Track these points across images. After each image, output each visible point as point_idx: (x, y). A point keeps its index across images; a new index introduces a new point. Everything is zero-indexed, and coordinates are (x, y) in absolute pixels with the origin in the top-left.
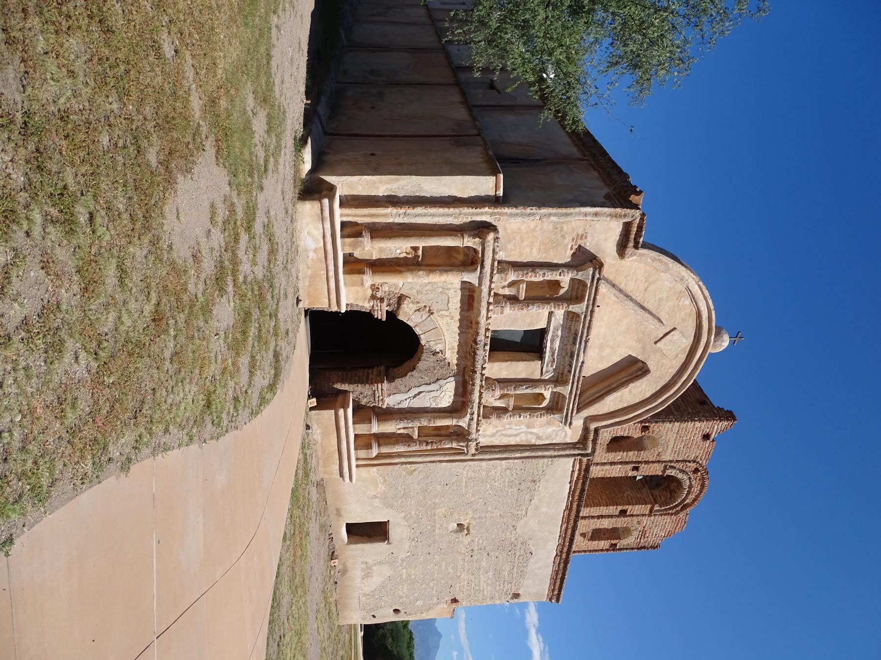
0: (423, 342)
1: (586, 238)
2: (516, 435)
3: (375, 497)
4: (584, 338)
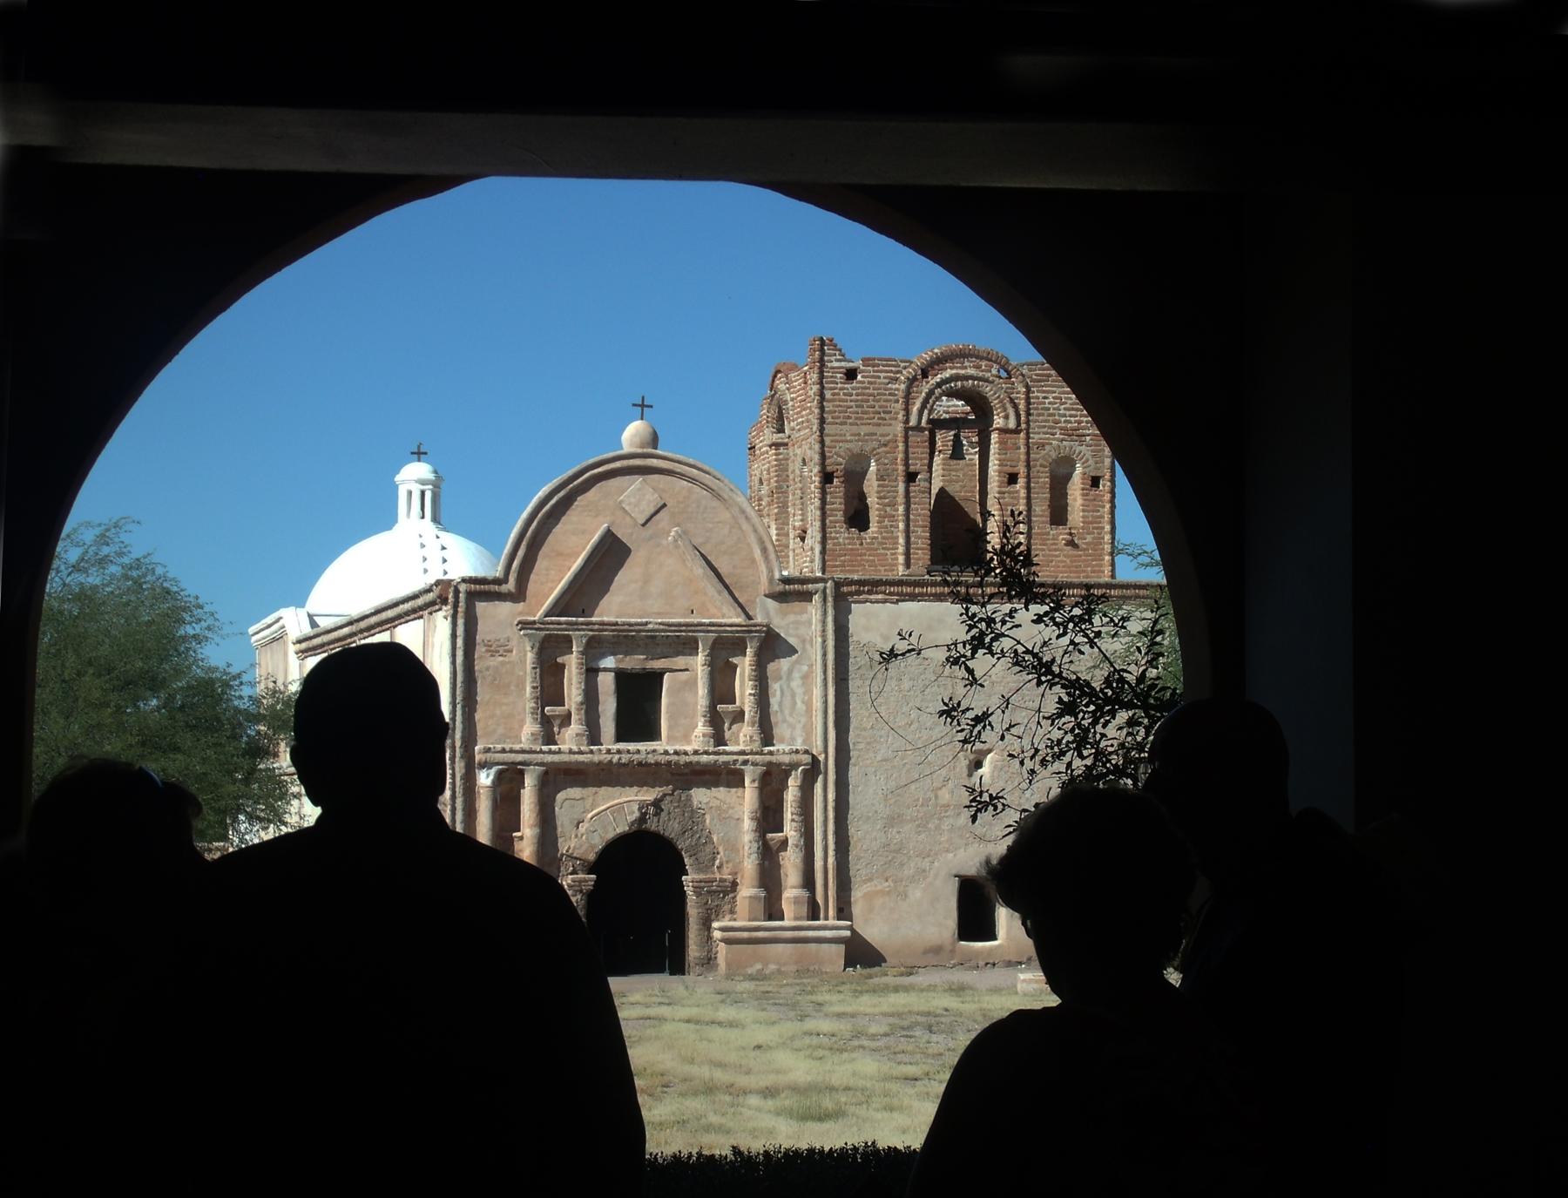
1: (489, 641)
2: (793, 695)
3: (905, 896)
4: (626, 627)
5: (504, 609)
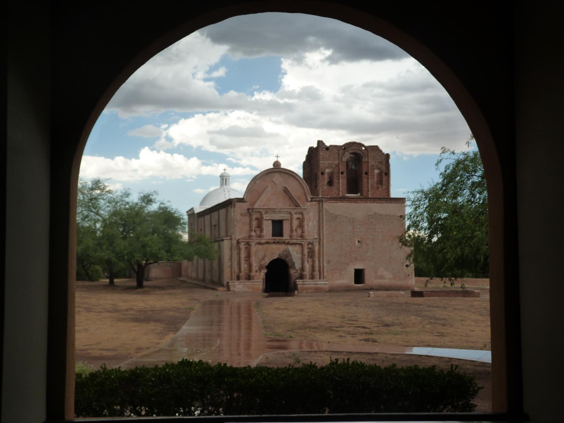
0: (276, 258)
5: (245, 206)
